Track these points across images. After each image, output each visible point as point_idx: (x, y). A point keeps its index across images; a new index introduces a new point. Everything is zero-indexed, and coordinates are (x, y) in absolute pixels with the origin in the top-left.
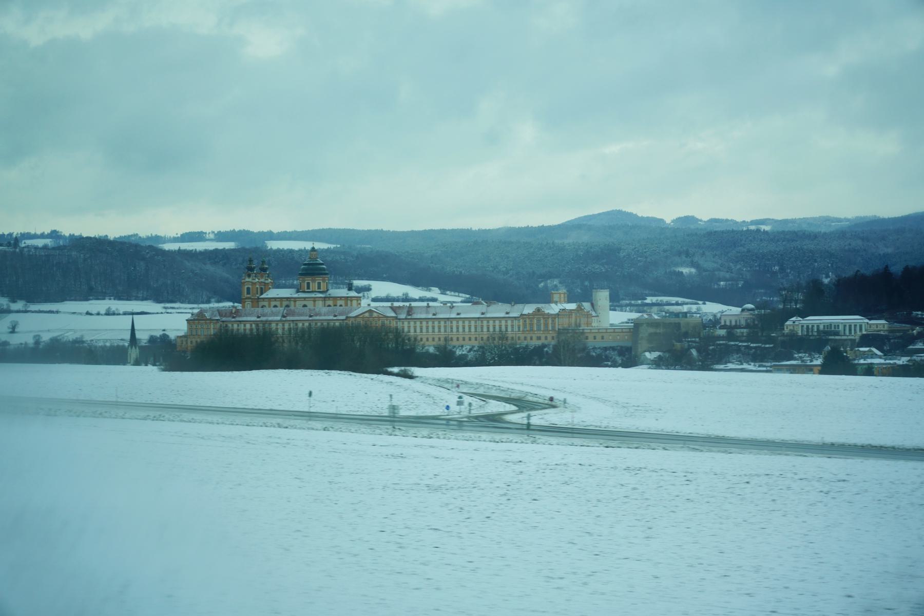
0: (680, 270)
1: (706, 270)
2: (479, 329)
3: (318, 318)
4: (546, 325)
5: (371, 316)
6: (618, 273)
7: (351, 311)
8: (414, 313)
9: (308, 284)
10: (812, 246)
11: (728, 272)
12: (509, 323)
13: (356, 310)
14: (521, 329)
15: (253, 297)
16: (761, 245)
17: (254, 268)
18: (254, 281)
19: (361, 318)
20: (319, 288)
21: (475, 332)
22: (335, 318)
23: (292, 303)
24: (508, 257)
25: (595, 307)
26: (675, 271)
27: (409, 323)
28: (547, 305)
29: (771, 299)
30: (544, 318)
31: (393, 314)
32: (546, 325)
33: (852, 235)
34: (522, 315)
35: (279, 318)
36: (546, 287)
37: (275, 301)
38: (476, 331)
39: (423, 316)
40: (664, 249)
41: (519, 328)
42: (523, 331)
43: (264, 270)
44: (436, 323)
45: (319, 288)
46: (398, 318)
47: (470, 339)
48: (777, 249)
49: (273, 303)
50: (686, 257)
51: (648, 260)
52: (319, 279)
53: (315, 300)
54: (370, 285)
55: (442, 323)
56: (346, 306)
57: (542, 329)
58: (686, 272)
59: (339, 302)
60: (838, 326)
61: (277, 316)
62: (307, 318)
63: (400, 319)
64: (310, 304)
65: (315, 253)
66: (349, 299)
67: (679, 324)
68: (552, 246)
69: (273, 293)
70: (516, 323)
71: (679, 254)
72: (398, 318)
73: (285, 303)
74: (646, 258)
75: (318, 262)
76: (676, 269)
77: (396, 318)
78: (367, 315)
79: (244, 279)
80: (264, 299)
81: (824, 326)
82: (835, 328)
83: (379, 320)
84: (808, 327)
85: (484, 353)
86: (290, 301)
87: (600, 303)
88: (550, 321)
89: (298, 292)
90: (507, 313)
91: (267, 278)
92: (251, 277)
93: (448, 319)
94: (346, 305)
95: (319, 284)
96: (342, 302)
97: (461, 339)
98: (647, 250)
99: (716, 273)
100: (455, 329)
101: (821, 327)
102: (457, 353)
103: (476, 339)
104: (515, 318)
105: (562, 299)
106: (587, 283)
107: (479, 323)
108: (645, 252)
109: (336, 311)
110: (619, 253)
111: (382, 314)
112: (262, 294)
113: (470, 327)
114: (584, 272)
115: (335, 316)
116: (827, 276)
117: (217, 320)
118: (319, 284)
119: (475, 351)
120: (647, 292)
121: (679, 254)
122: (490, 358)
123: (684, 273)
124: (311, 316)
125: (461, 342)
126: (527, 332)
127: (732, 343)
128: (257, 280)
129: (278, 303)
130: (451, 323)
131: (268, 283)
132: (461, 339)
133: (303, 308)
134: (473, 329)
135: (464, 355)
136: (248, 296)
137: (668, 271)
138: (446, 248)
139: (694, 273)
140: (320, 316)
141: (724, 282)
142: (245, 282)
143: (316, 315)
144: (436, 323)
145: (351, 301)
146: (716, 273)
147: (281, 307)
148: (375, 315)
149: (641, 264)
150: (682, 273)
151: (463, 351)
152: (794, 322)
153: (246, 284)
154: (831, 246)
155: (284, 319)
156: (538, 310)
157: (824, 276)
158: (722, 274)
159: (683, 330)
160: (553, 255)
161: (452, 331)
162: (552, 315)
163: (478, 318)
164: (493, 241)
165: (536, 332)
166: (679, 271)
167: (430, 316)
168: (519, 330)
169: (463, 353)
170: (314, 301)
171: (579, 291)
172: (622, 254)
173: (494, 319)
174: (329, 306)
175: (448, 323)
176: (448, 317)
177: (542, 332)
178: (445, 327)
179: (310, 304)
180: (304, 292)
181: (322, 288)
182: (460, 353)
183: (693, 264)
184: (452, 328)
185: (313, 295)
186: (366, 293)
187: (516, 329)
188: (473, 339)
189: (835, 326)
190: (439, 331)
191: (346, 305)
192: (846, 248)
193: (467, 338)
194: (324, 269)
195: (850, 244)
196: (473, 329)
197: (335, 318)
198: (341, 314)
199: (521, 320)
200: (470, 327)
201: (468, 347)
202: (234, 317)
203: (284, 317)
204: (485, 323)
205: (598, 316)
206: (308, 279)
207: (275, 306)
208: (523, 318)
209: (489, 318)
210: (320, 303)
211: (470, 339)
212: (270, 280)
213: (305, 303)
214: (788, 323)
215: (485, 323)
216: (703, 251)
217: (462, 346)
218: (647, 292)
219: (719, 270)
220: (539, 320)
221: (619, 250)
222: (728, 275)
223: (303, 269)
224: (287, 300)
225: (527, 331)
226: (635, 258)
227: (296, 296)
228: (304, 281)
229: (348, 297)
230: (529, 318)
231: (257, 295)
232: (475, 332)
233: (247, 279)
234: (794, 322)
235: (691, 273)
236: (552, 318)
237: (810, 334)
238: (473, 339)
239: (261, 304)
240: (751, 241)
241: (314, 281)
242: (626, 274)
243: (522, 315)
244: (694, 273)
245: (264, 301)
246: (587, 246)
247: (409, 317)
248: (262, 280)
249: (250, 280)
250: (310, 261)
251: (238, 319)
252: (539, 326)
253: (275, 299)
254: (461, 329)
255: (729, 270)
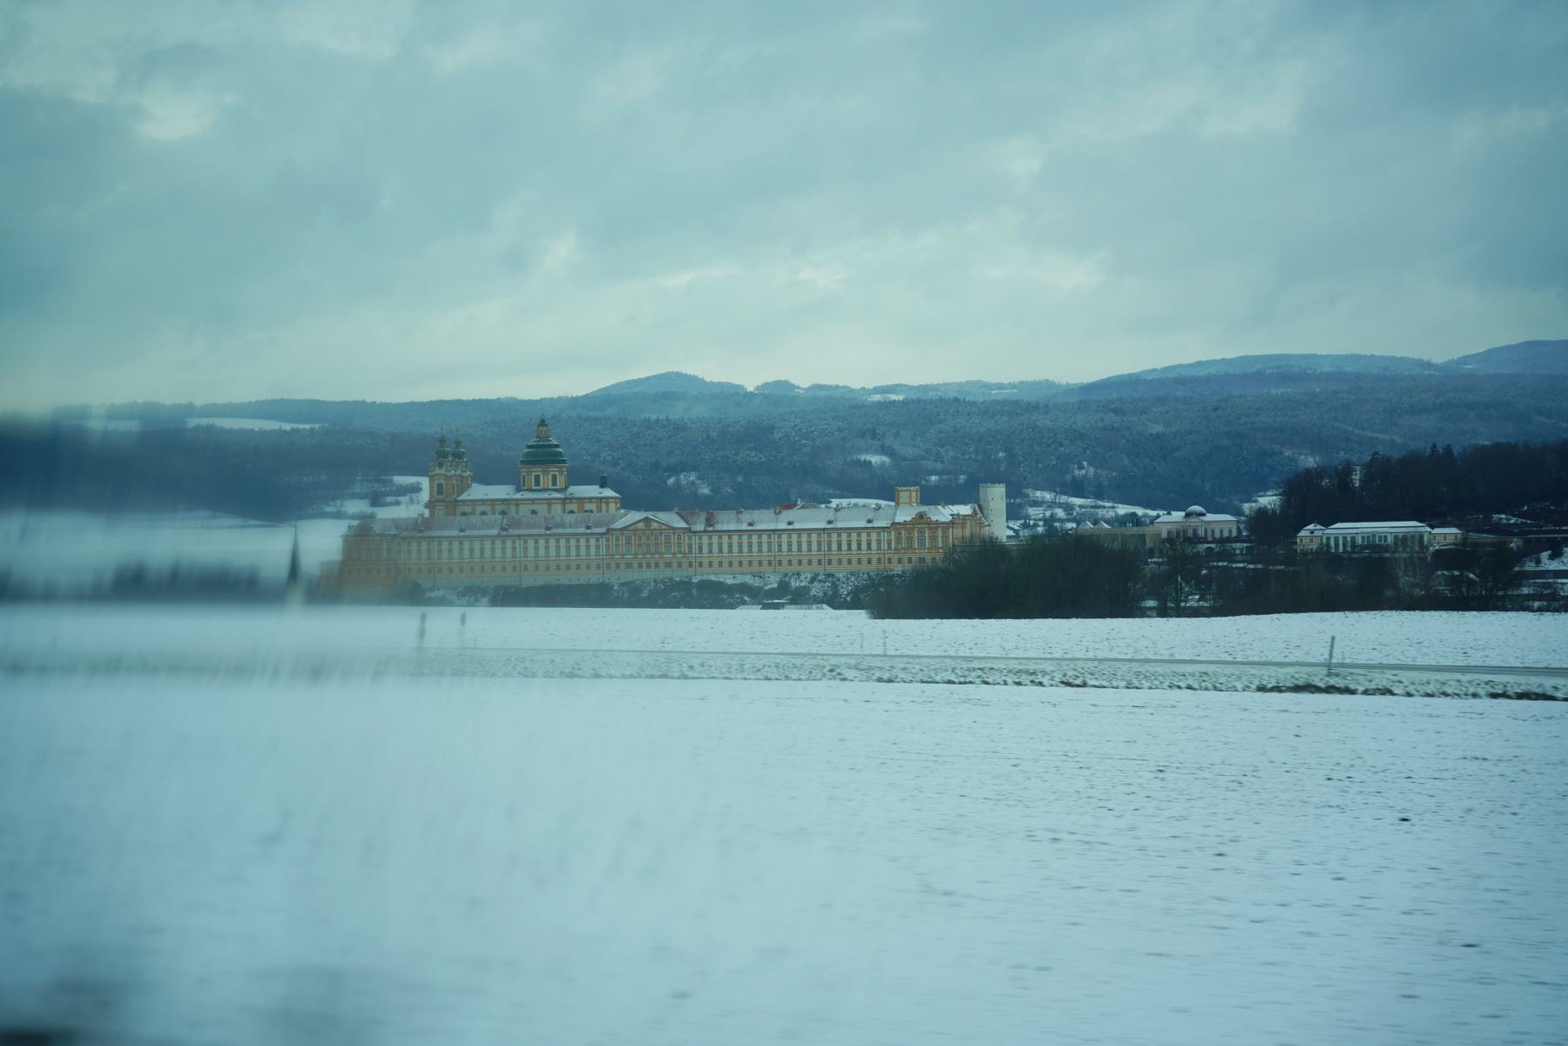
0: (868, 459)
1: (906, 459)
2: (824, 547)
3: (560, 531)
4: (934, 538)
5: (648, 527)
6: (785, 464)
7: (614, 520)
8: (718, 522)
9: (537, 478)
10: (1048, 422)
11: (936, 461)
12: (874, 536)
13: (621, 518)
14: (893, 547)
15: (447, 499)
16: (971, 421)
17: (448, 452)
18: (449, 474)
19: (633, 530)
20: (554, 483)
21: (596, 555)
22: (588, 531)
23: (513, 508)
24: (599, 441)
25: (985, 512)
26: (859, 461)
27: (710, 538)
28: (932, 507)
29: (1012, 501)
30: (930, 529)
31: (683, 525)
32: (934, 538)
33: (1098, 406)
34: (894, 524)
35: (495, 532)
36: (678, 483)
37: (483, 504)
38: (819, 550)
39: (733, 527)
40: (838, 428)
41: (889, 544)
42: (896, 549)
43: (459, 456)
44: (755, 538)
45: (554, 483)
46: (693, 529)
47: (810, 562)
48: (999, 427)
49: (480, 509)
50: (873, 439)
51: (817, 443)
52: (554, 470)
53: (549, 502)
54: (419, 484)
55: (765, 538)
56: (598, 512)
57: (927, 546)
58: (876, 462)
59: (588, 506)
60: (1386, 537)
61: (492, 528)
62: (542, 531)
63: (695, 532)
64: (542, 509)
65: (545, 428)
66: (604, 500)
67: (1144, 535)
68: (666, 423)
69: (478, 492)
70: (884, 536)
71: (862, 434)
72: (693, 529)
73: (499, 508)
74: (813, 440)
75: (551, 443)
76: (859, 457)
77: (689, 530)
78: (641, 525)
79: (433, 471)
80: (464, 501)
81: (1363, 538)
82: (1380, 540)
83: (661, 534)
84: (1345, 539)
85: (835, 587)
86: (507, 504)
87: (992, 505)
88: (940, 532)
89: (518, 490)
90: (869, 521)
91: (464, 469)
92: (445, 467)
93: (774, 531)
94: (599, 510)
95: (554, 477)
96: (593, 506)
97: (795, 562)
98: (813, 429)
99: (922, 462)
100: (785, 547)
101: (1359, 541)
102: (793, 584)
103: (820, 562)
104: (883, 528)
105: (914, 500)
106: (740, 479)
107: (824, 537)
108: (812, 433)
109: (589, 520)
110: (772, 433)
111: (665, 525)
112: (458, 495)
113: (809, 543)
114: (735, 462)
115: (588, 528)
116: (1081, 467)
117: (394, 535)
118: (554, 477)
119: (820, 581)
120: (831, 491)
121: (862, 434)
122: (845, 593)
123: (873, 463)
124: (548, 528)
125: (795, 568)
126: (903, 551)
127: (1280, 567)
128: (453, 472)
129: (487, 508)
130: (780, 537)
131: (467, 477)
132: (795, 562)
133: (533, 516)
134: (815, 547)
135: (804, 587)
136: (440, 497)
137: (848, 460)
138: (499, 427)
139: (887, 464)
140: (564, 528)
141: (937, 477)
142: (434, 475)
143: (557, 526)
144: (794, 537)
145: (607, 504)
146: (922, 462)
147: (493, 513)
148: (654, 525)
149: (807, 449)
150: (870, 462)
151: (801, 581)
152: (1312, 533)
153: (435, 478)
154: (1075, 422)
155: (504, 533)
156: (921, 516)
157: (1076, 466)
158: (929, 464)
159: (1149, 544)
160: (669, 437)
161: (780, 550)
162: (944, 523)
163: (824, 529)
164: (569, 417)
165: (917, 551)
166: (865, 460)
167: (745, 527)
168: (889, 548)
169: (802, 584)
170: (549, 505)
171: (730, 490)
172: (777, 435)
173: (849, 530)
174: (572, 512)
175: (775, 538)
176: (773, 528)
177: (926, 551)
178: (769, 543)
179: (542, 509)
180: (530, 490)
181: (558, 484)
182: (798, 585)
183: (884, 450)
184: (780, 546)
185: (546, 495)
186: (414, 496)
187: (884, 546)
188: (815, 562)
189: (1380, 537)
190: (760, 550)
191: (599, 510)
192: (1100, 424)
193: (805, 562)
194: (560, 454)
195: (1103, 420)
196: (815, 547)
197: (588, 531)
198: (597, 525)
199: (893, 532)
200: (809, 543)
201: (809, 576)
202: (420, 531)
203: (504, 529)
204: (834, 537)
205: (989, 525)
206: (537, 470)
207: (483, 513)
208: (896, 530)
209: (841, 529)
210: (558, 508)
211: (810, 562)
212: (468, 473)
213: (535, 507)
214: (1302, 533)
215: (834, 537)
216: (897, 431)
217: (799, 574)
218: (831, 491)
219: (924, 458)
220: (921, 532)
221: (772, 428)
222: (939, 466)
223: (527, 455)
224: (503, 504)
225: (903, 549)
226: (796, 441)
227: (518, 496)
228: (529, 473)
229: (602, 498)
230: (906, 529)
231: (454, 496)
232: (596, 555)
233: (438, 471)
234: (1312, 533)
235: (883, 464)
236: (943, 528)
237: (1341, 550)
238: (815, 562)
239: (460, 509)
240: (953, 415)
241: (546, 473)
242: (798, 464)
243: (894, 524)
244: (887, 464)
245: (464, 504)
246: (720, 422)
247: (711, 529)
248: (458, 472)
249: (443, 471)
250: (539, 441)
251: (428, 534)
252: (921, 541)
253: (483, 501)
254: (795, 548)
255: (939, 458)
